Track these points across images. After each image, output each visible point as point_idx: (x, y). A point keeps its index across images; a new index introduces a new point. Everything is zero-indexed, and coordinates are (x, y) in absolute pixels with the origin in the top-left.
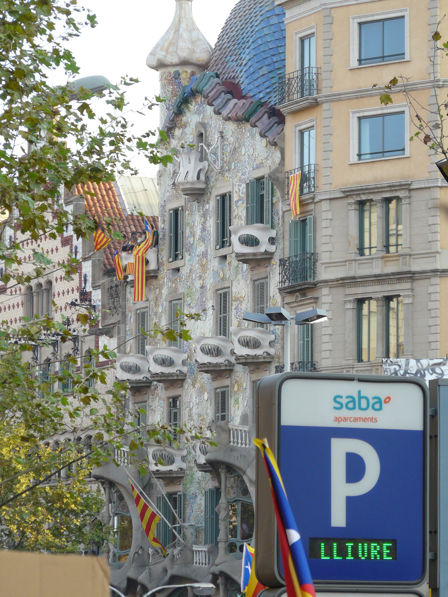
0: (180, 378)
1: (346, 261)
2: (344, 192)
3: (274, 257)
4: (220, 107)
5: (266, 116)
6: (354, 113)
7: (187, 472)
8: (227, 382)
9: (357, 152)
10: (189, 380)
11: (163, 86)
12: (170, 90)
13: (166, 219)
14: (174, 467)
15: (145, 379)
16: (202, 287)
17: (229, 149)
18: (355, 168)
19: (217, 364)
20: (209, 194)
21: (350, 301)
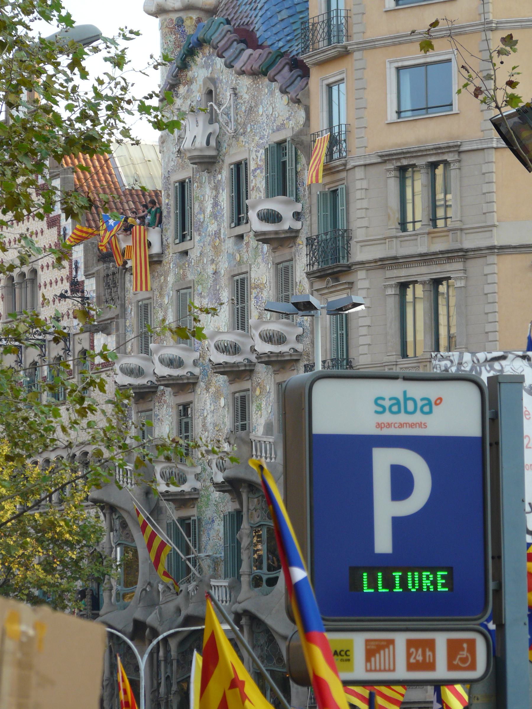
0: (191, 381)
1: (385, 239)
2: (381, 156)
3: (300, 235)
4: (232, 58)
5: (287, 68)
6: (391, 62)
7: (202, 493)
8: (247, 385)
9: (395, 108)
10: (202, 383)
11: (164, 36)
12: (172, 40)
13: (170, 193)
14: (186, 487)
15: (149, 384)
16: (215, 273)
17: (244, 108)
18: (394, 128)
19: (234, 363)
20: (221, 162)
21: (391, 286)
